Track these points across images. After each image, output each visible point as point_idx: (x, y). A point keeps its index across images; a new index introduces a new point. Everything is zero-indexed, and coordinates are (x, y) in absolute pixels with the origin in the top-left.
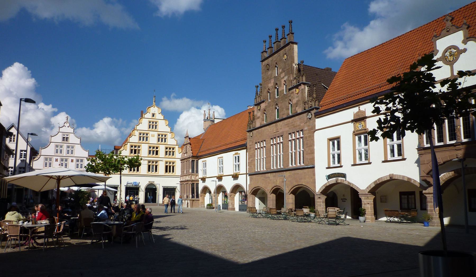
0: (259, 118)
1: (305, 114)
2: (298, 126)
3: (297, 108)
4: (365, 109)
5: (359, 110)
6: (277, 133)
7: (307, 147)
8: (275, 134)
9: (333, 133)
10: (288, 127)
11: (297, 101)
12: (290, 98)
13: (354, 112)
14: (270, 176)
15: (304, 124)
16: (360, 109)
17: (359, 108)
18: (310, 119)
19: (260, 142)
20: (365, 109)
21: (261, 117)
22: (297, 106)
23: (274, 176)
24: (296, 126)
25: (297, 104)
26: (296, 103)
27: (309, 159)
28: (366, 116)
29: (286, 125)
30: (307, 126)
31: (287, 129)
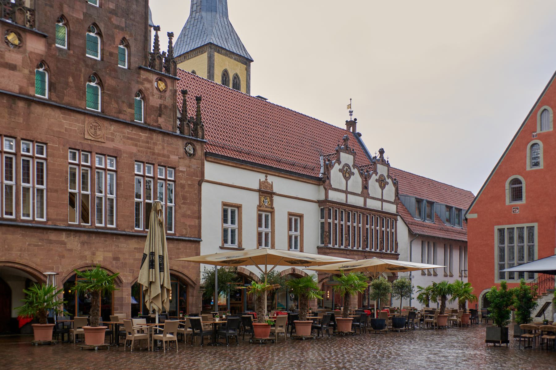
0: (13, 67)
1: (180, 144)
2: (164, 156)
3: (161, 120)
4: (272, 182)
5: (266, 180)
6: (95, 144)
7: (184, 203)
8: (90, 145)
9: (234, 197)
10: (136, 145)
11: (161, 105)
12: (141, 87)
13: (260, 180)
14: (66, 240)
15: (177, 157)
16: (267, 180)
17: (266, 177)
18: (190, 155)
19: (19, 138)
20: (272, 182)
21: (26, 71)
22: (160, 115)
23: (83, 243)
24: (159, 155)
25: (160, 111)
26: (157, 107)
27: (187, 226)
28: (274, 192)
29: (129, 138)
30: (185, 166)
31: (134, 150)
